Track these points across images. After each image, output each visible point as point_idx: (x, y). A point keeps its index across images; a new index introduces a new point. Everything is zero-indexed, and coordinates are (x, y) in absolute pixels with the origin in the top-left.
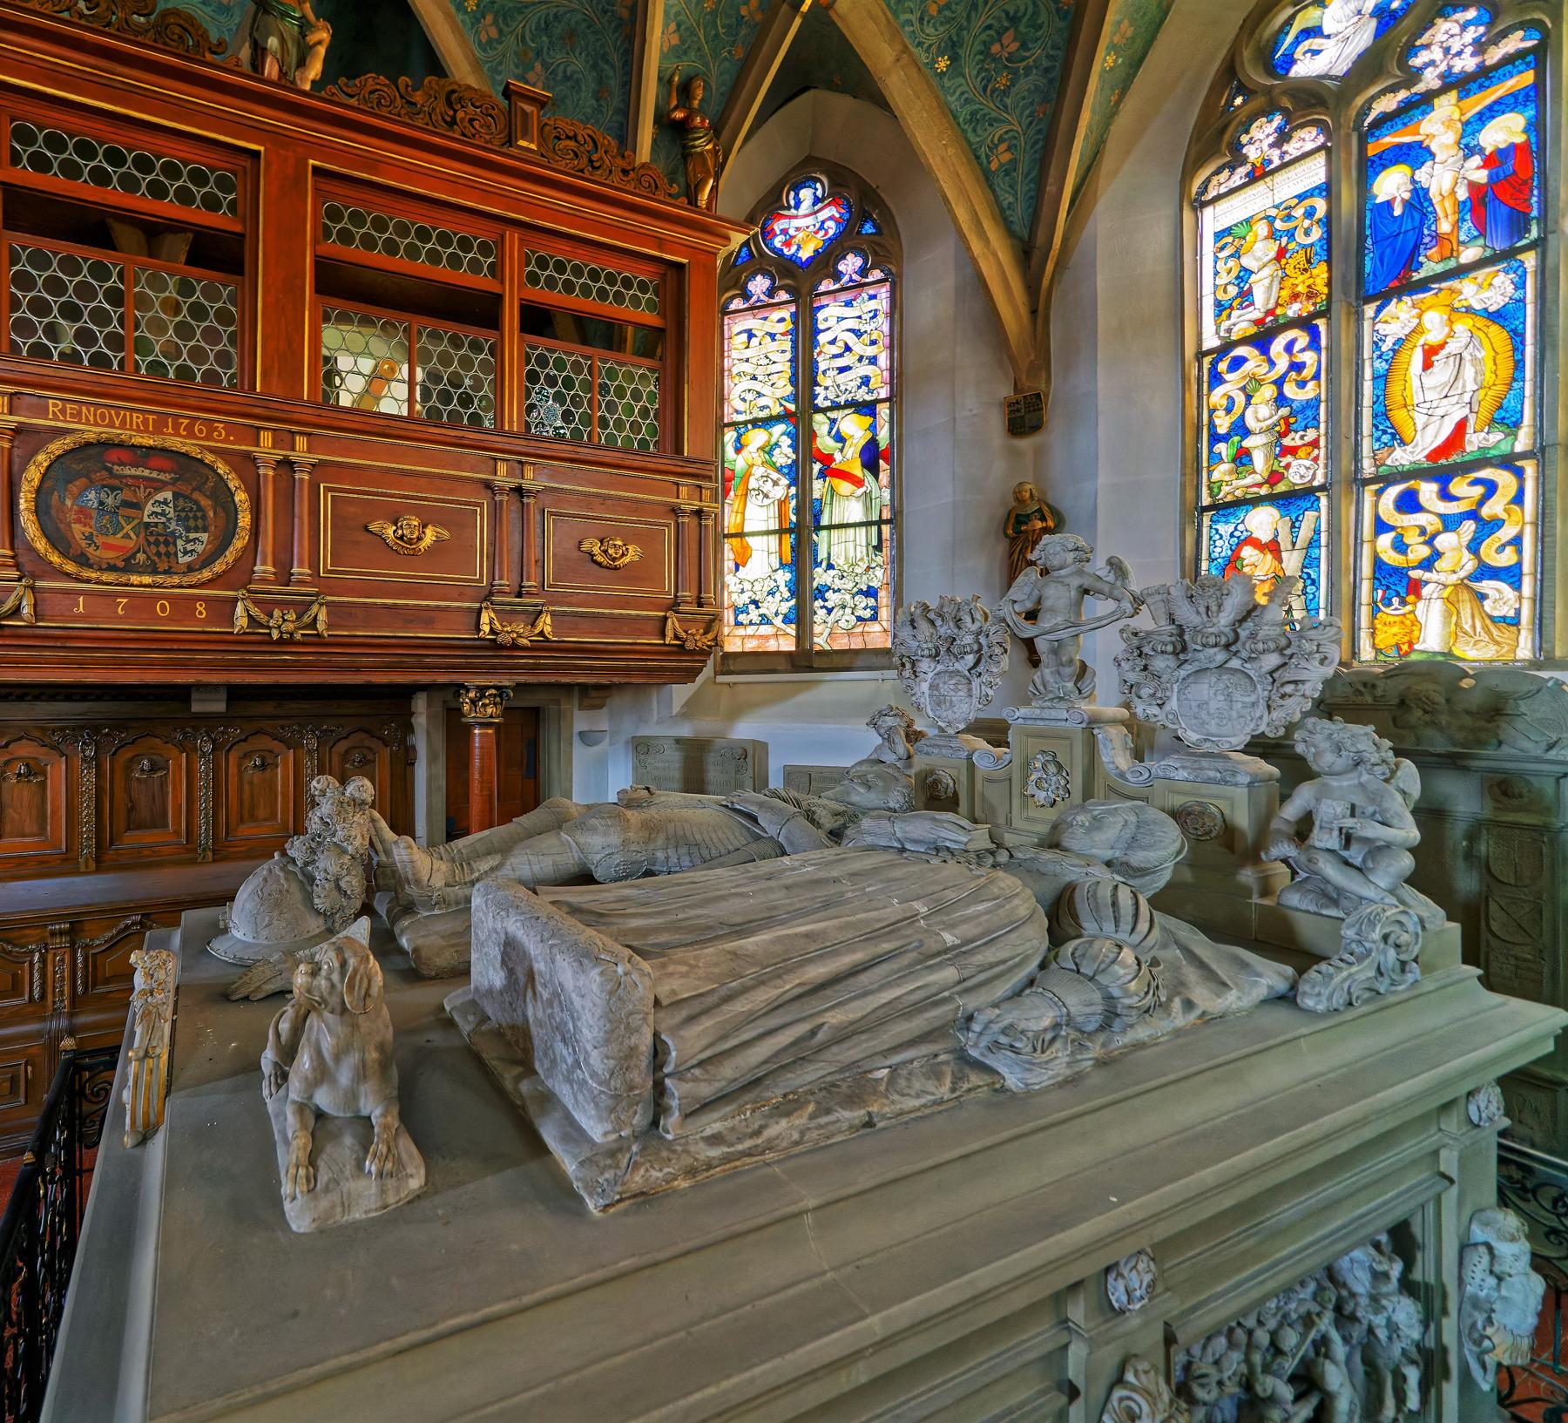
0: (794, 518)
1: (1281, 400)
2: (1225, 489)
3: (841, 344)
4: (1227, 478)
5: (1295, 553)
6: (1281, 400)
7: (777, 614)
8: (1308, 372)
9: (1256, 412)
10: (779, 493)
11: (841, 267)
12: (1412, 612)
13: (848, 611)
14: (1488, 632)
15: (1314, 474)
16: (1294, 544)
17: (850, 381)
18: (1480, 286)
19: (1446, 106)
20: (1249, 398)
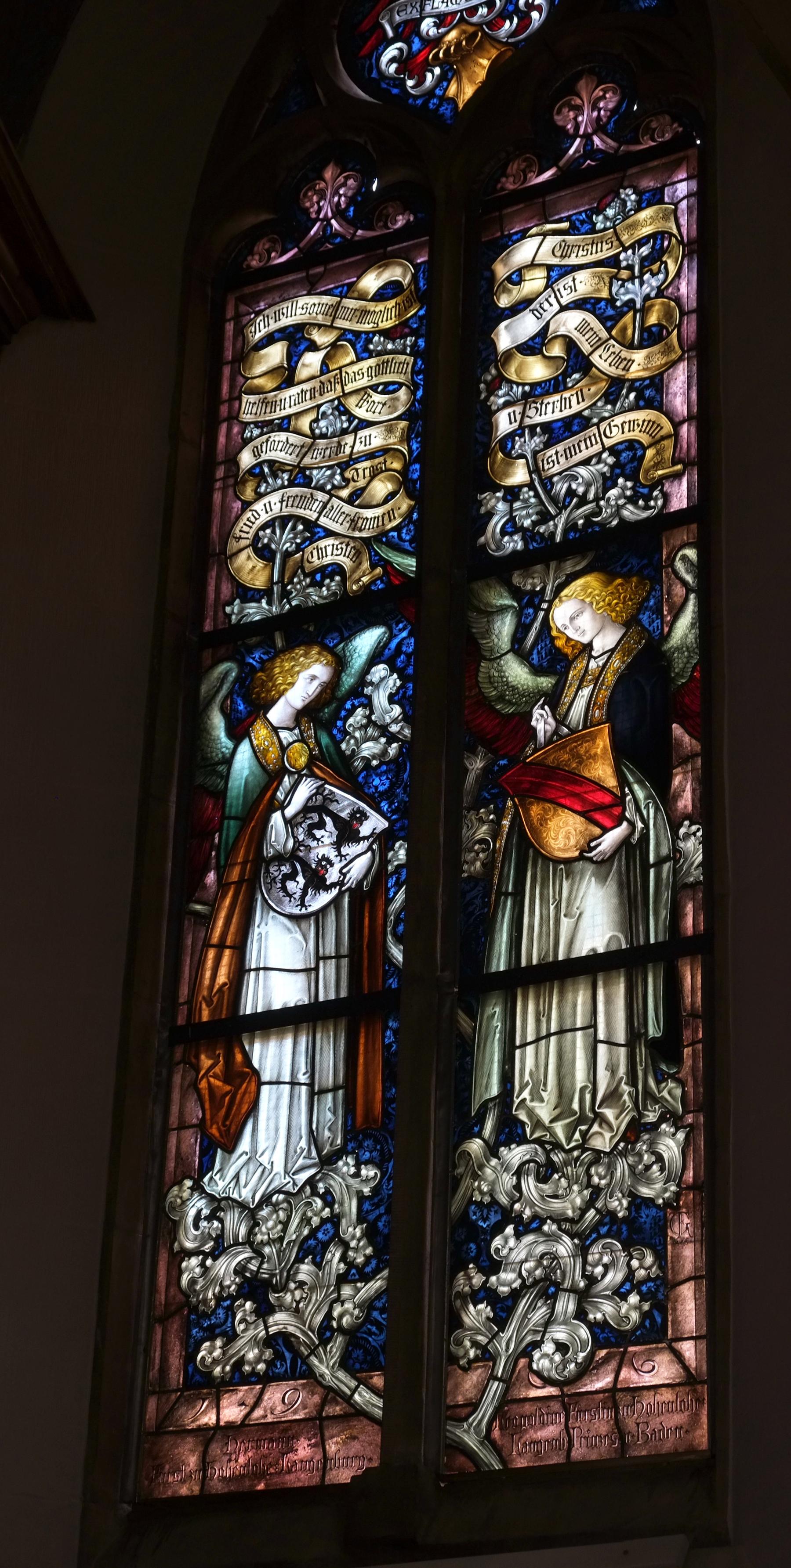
0: (397, 953)
3: (557, 350)
7: (326, 1332)
10: (358, 863)
11: (565, 119)
13: (566, 1305)
17: (577, 465)
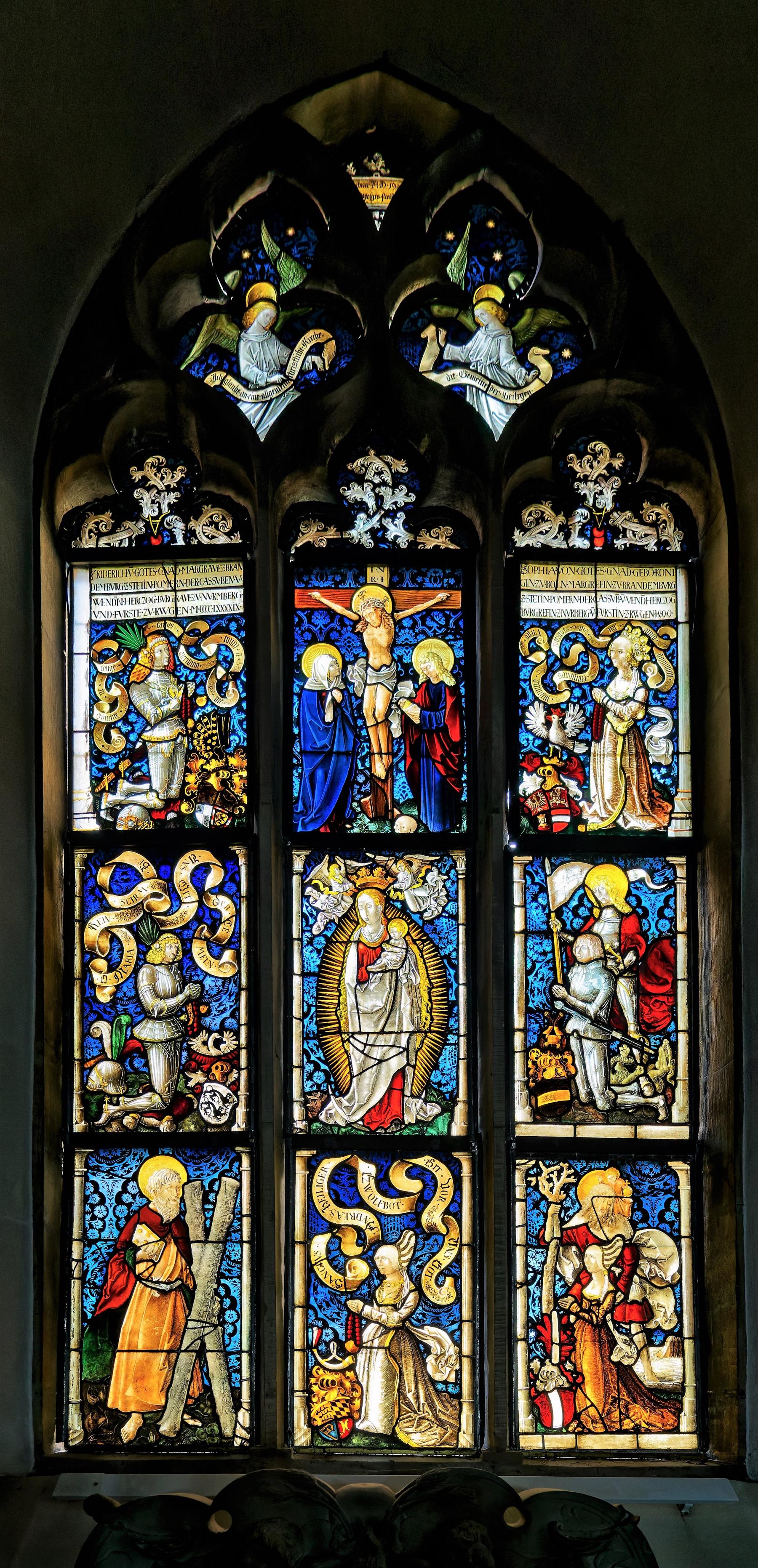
1: (185, 968)
2: (109, 1109)
4: (111, 1089)
5: (210, 1248)
6: (185, 968)
8: (224, 931)
9: (153, 979)
12: (352, 1367)
14: (432, 1406)
15: (233, 1113)
16: (207, 1231)
18: (415, 876)
19: (379, 574)
20: (143, 950)
